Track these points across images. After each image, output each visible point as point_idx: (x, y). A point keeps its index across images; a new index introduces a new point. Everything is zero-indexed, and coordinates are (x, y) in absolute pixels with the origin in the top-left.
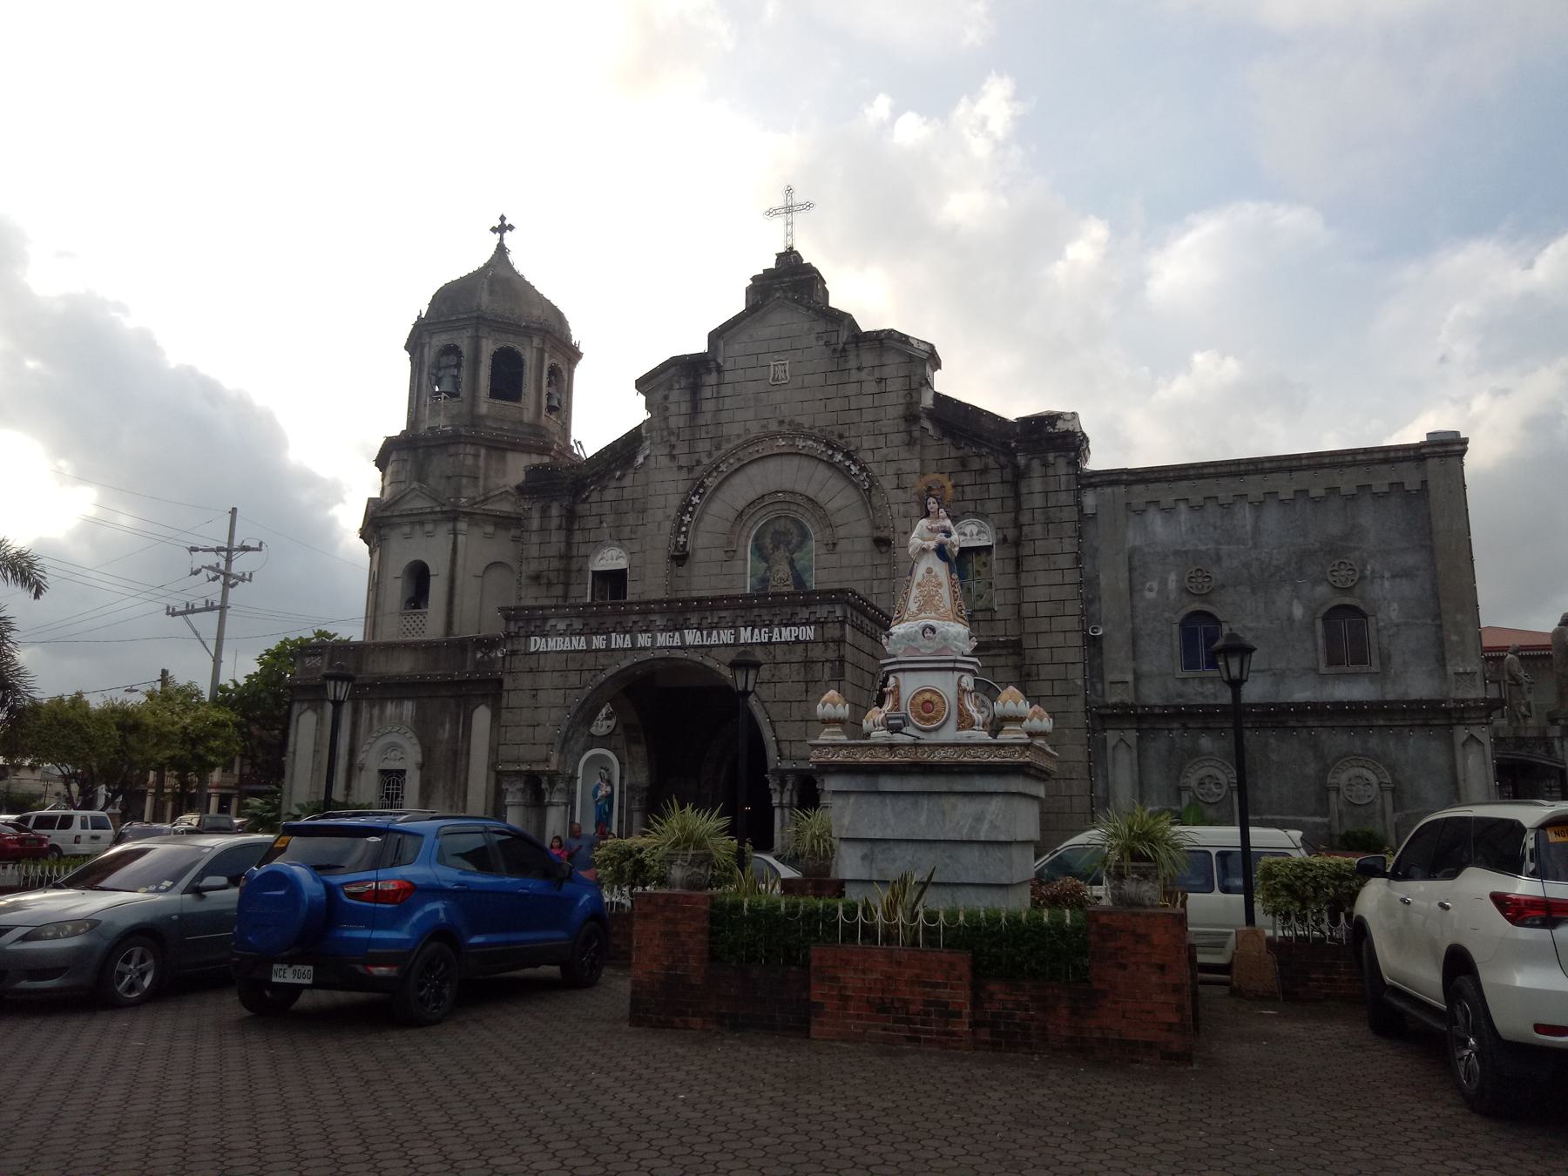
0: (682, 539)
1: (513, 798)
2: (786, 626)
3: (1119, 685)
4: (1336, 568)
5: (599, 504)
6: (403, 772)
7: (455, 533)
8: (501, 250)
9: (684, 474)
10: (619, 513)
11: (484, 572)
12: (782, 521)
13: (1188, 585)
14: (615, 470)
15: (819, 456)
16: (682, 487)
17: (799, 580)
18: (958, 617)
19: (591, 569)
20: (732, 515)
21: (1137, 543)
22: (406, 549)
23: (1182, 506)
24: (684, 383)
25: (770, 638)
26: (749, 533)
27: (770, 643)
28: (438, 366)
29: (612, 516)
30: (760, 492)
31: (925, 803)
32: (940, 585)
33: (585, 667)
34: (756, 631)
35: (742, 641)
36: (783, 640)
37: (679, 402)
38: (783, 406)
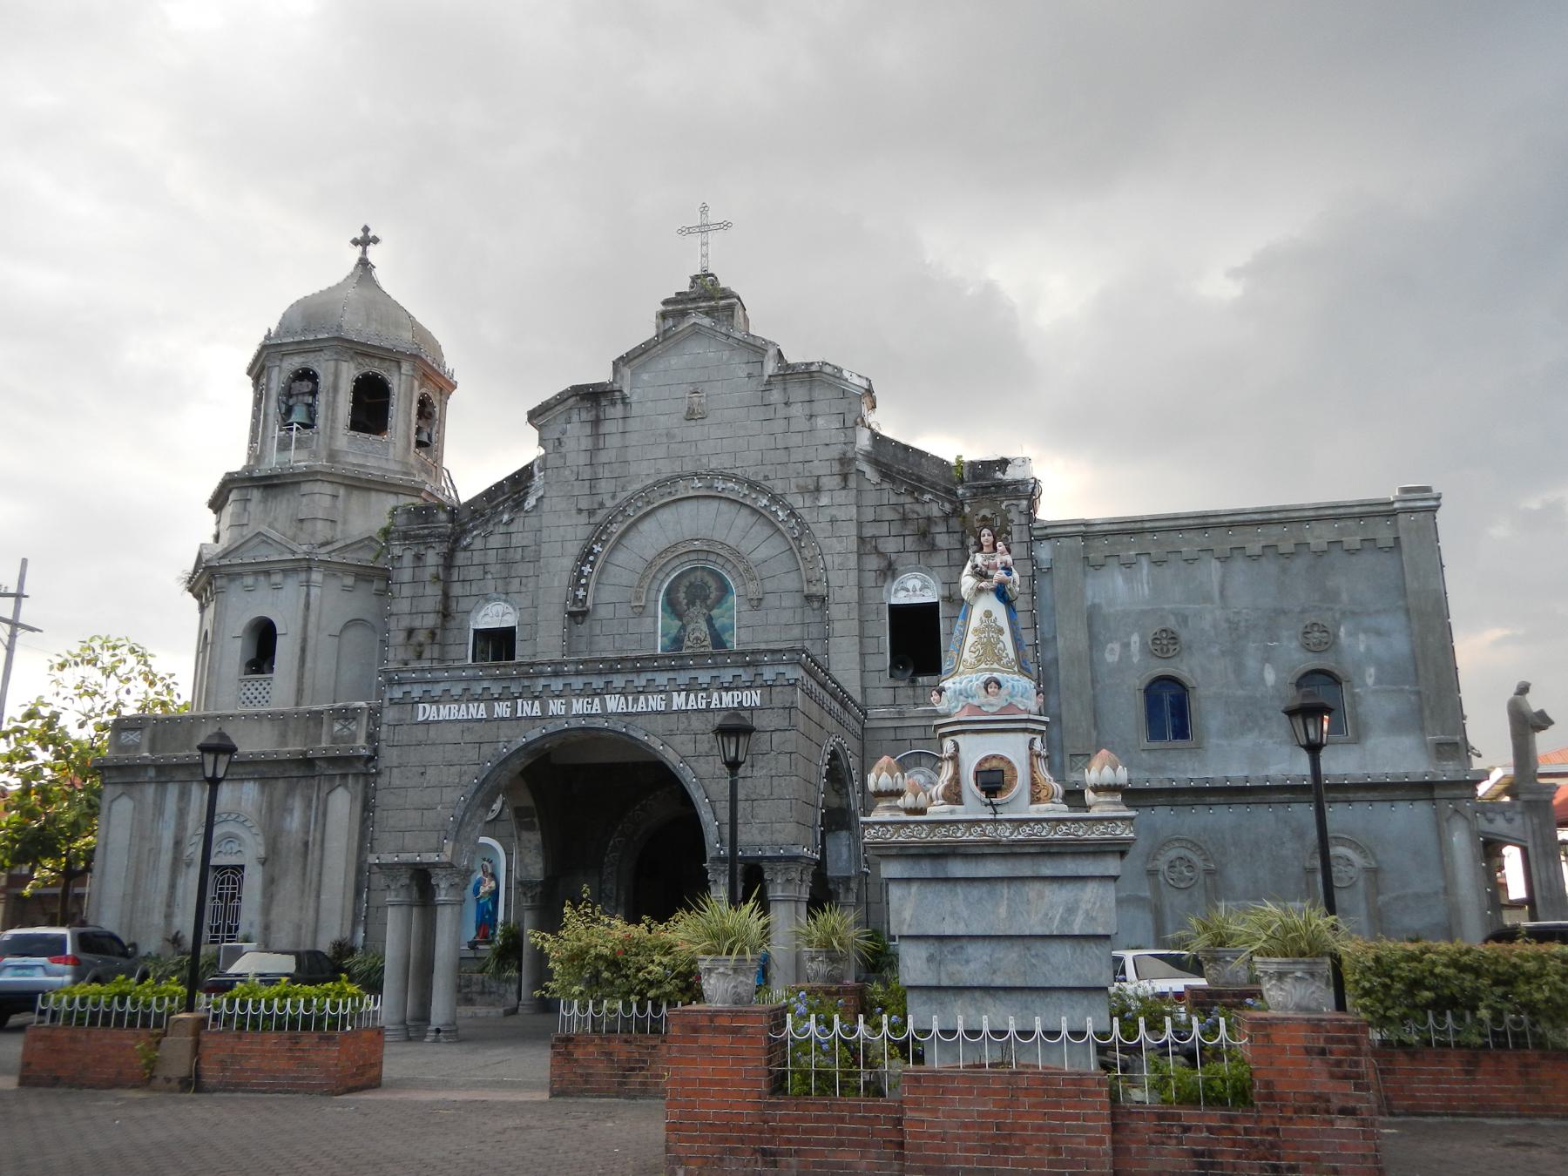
0: (581, 593)
1: (397, 896)
2: (727, 689)
3: (1080, 758)
4: (1308, 630)
6: (242, 867)
7: (308, 584)
8: (364, 264)
9: (583, 518)
10: (508, 563)
11: (341, 631)
12: (699, 573)
13: (1152, 648)
14: (502, 513)
15: (741, 500)
16: (583, 532)
17: (718, 641)
18: (1024, 670)
19: (472, 627)
20: (640, 566)
21: (1097, 601)
22: (246, 606)
23: (1144, 561)
24: (585, 416)
25: (709, 704)
26: (661, 585)
27: (708, 710)
28: (288, 393)
29: (498, 566)
30: (673, 541)
31: (1004, 890)
32: (1001, 631)
33: (486, 739)
34: (692, 696)
35: (675, 708)
36: (724, 706)
37: (576, 432)
38: (699, 443)
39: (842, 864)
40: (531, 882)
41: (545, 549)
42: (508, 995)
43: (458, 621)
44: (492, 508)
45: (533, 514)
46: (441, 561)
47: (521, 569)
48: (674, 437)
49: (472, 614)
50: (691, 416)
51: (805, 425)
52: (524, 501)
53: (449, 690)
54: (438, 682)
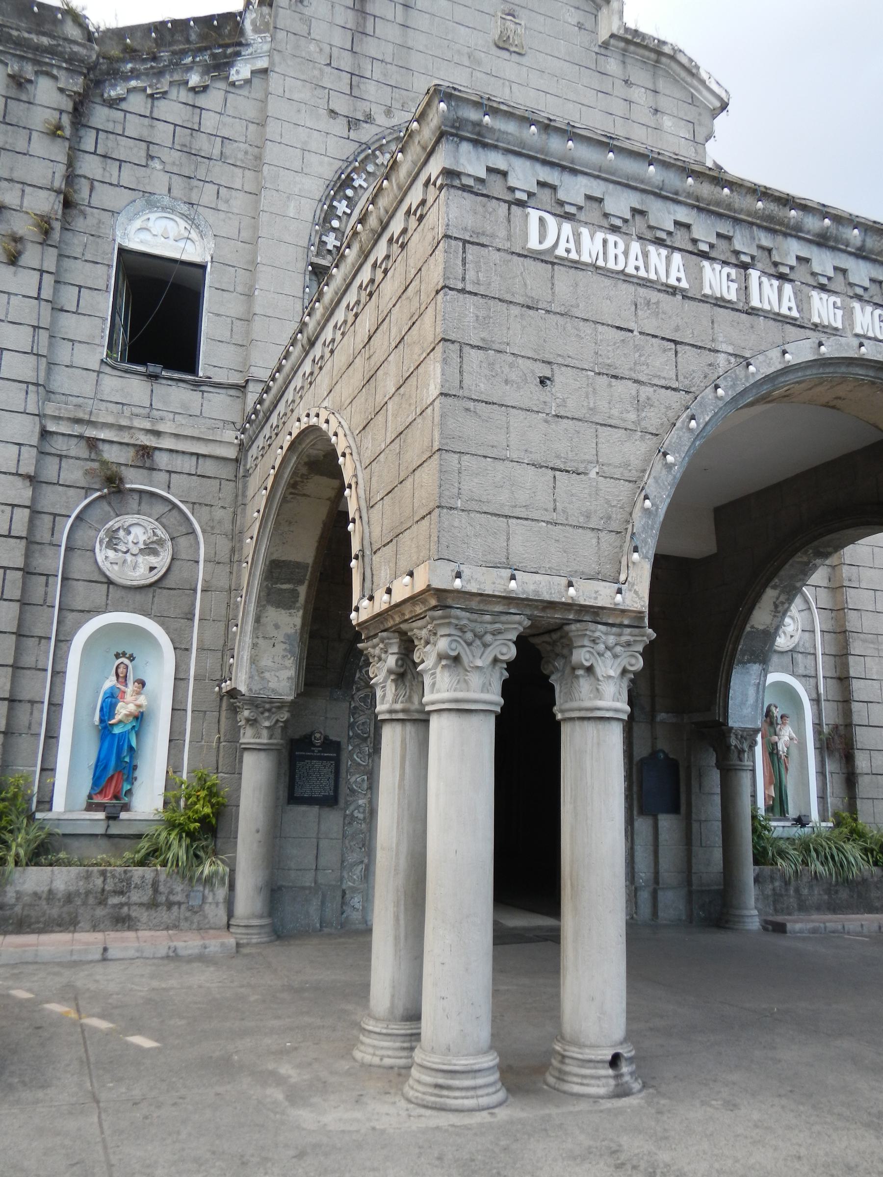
5: (146, 121)
9: (339, 127)
14: (189, 69)
19: (119, 240)
39: (747, 711)
40: (271, 701)
41: (272, 153)
42: (207, 907)
43: (91, 221)
44: (174, 53)
45: (244, 92)
46: (68, 105)
47: (219, 172)
48: (479, 63)
49: (121, 219)
50: (503, 45)
51: (649, 119)
52: (230, 65)
53: (600, 201)
54: (574, 172)
